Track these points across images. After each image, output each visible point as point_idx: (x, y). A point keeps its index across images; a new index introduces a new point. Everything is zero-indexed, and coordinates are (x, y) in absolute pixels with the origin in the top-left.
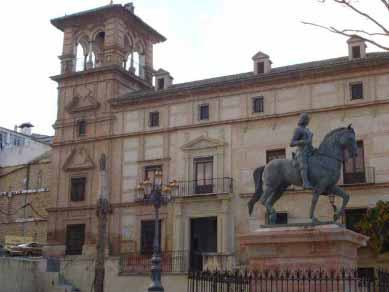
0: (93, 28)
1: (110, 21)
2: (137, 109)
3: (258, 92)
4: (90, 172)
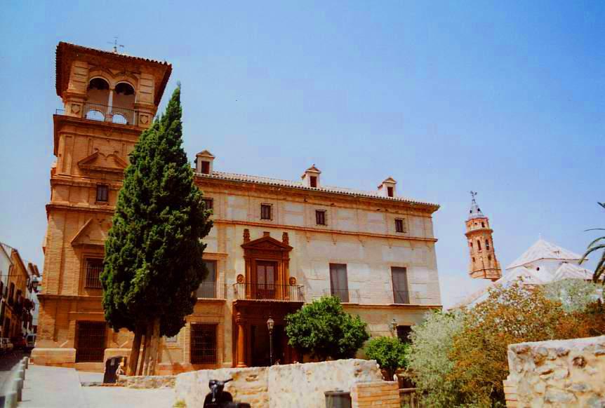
0: (117, 75)
1: (144, 75)
3: (321, 205)
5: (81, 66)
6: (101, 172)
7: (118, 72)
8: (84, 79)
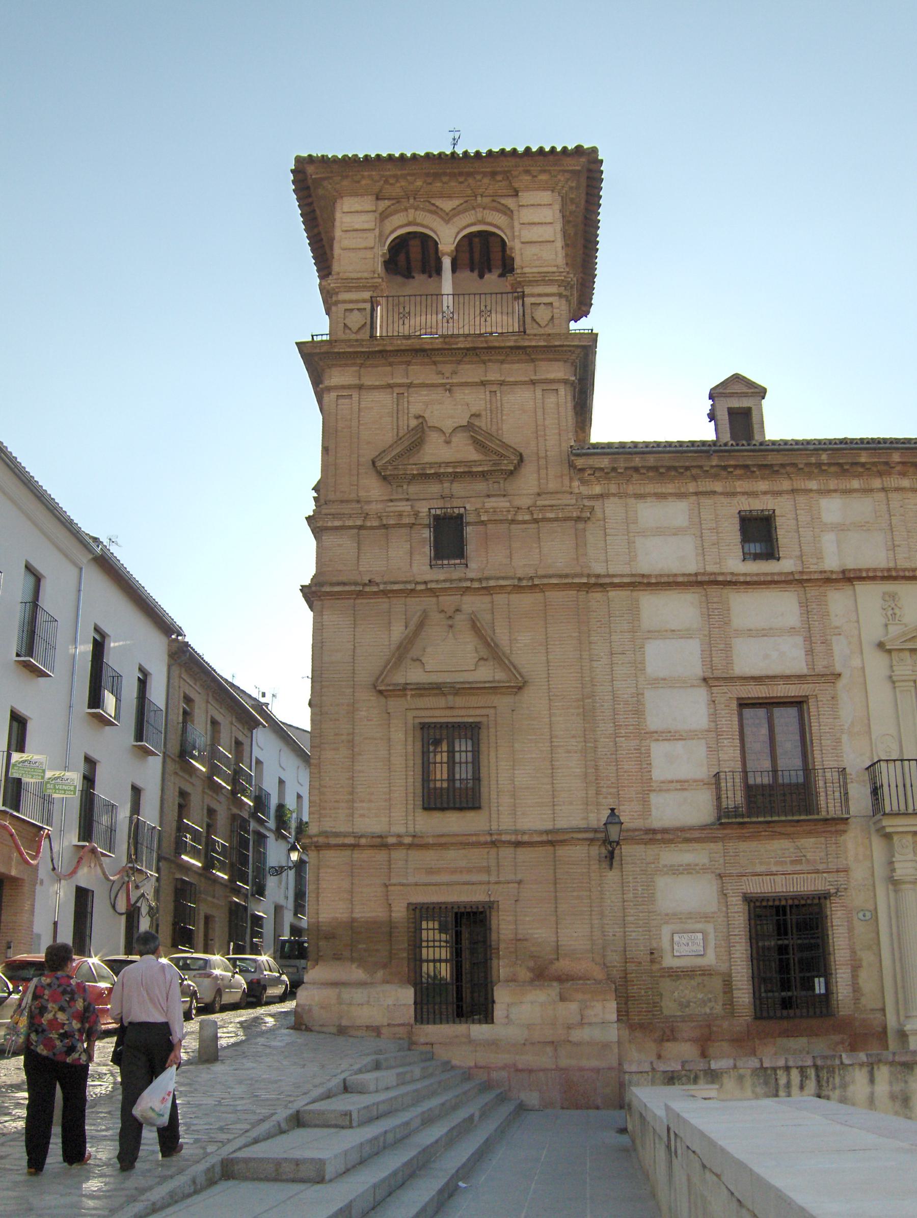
0: (456, 212)
1: (526, 197)
2: (681, 496)
4: (503, 702)
5: (359, 208)
6: (438, 477)
7: (455, 203)
8: (370, 240)
